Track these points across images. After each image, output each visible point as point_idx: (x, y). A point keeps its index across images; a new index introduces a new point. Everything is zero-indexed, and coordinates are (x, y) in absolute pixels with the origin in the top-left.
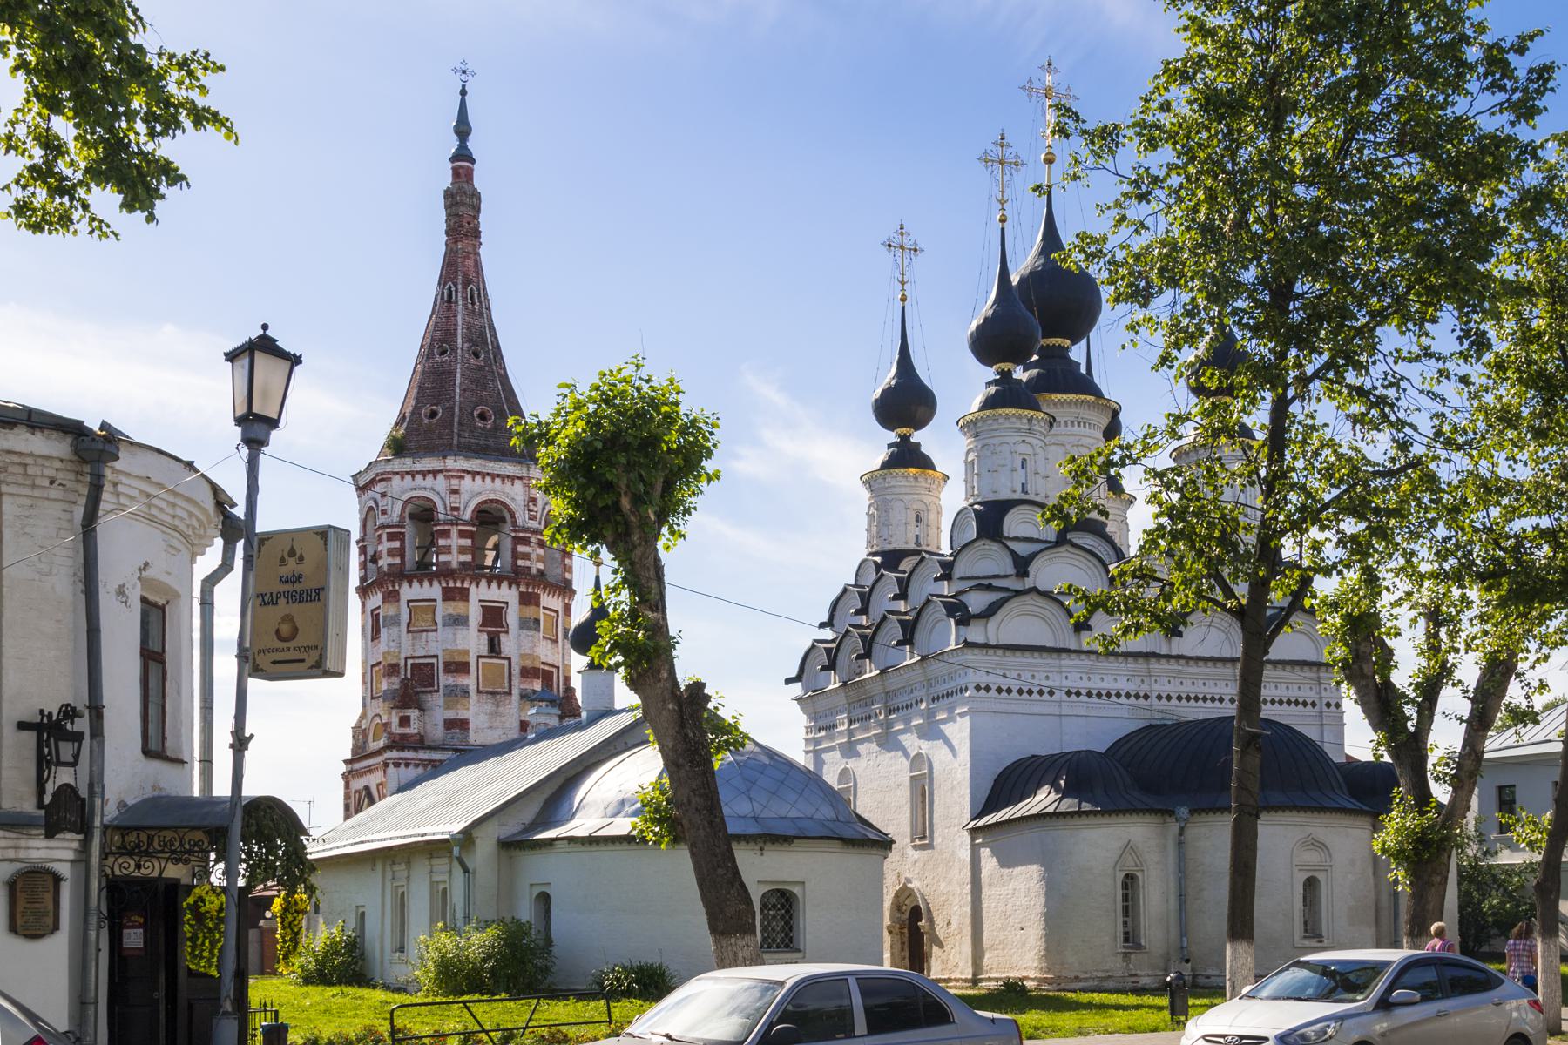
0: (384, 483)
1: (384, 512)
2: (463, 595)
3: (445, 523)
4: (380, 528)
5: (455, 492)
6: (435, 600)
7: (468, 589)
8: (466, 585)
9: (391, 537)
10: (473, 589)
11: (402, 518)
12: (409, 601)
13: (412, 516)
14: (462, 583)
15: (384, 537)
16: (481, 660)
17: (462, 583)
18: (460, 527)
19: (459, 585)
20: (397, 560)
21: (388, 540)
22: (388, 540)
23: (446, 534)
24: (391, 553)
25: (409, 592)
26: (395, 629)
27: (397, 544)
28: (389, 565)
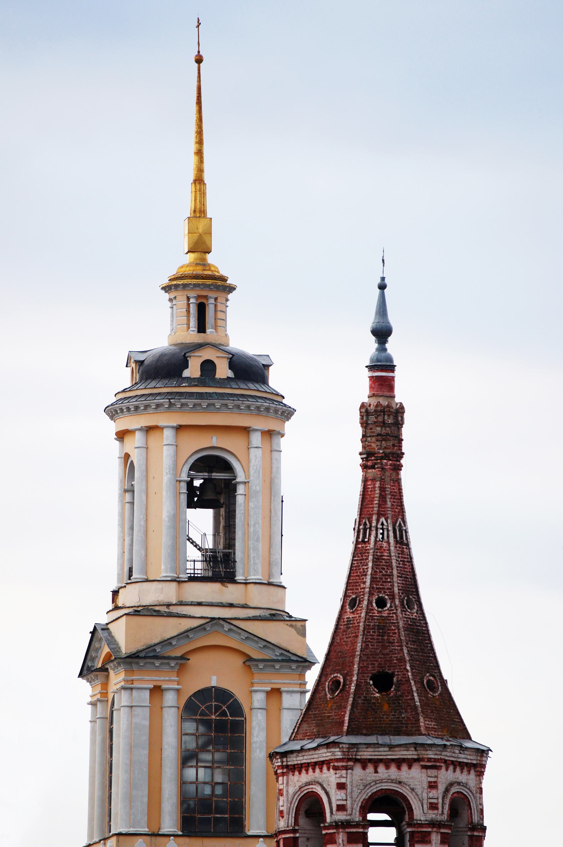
3: (330, 827)
5: (341, 786)
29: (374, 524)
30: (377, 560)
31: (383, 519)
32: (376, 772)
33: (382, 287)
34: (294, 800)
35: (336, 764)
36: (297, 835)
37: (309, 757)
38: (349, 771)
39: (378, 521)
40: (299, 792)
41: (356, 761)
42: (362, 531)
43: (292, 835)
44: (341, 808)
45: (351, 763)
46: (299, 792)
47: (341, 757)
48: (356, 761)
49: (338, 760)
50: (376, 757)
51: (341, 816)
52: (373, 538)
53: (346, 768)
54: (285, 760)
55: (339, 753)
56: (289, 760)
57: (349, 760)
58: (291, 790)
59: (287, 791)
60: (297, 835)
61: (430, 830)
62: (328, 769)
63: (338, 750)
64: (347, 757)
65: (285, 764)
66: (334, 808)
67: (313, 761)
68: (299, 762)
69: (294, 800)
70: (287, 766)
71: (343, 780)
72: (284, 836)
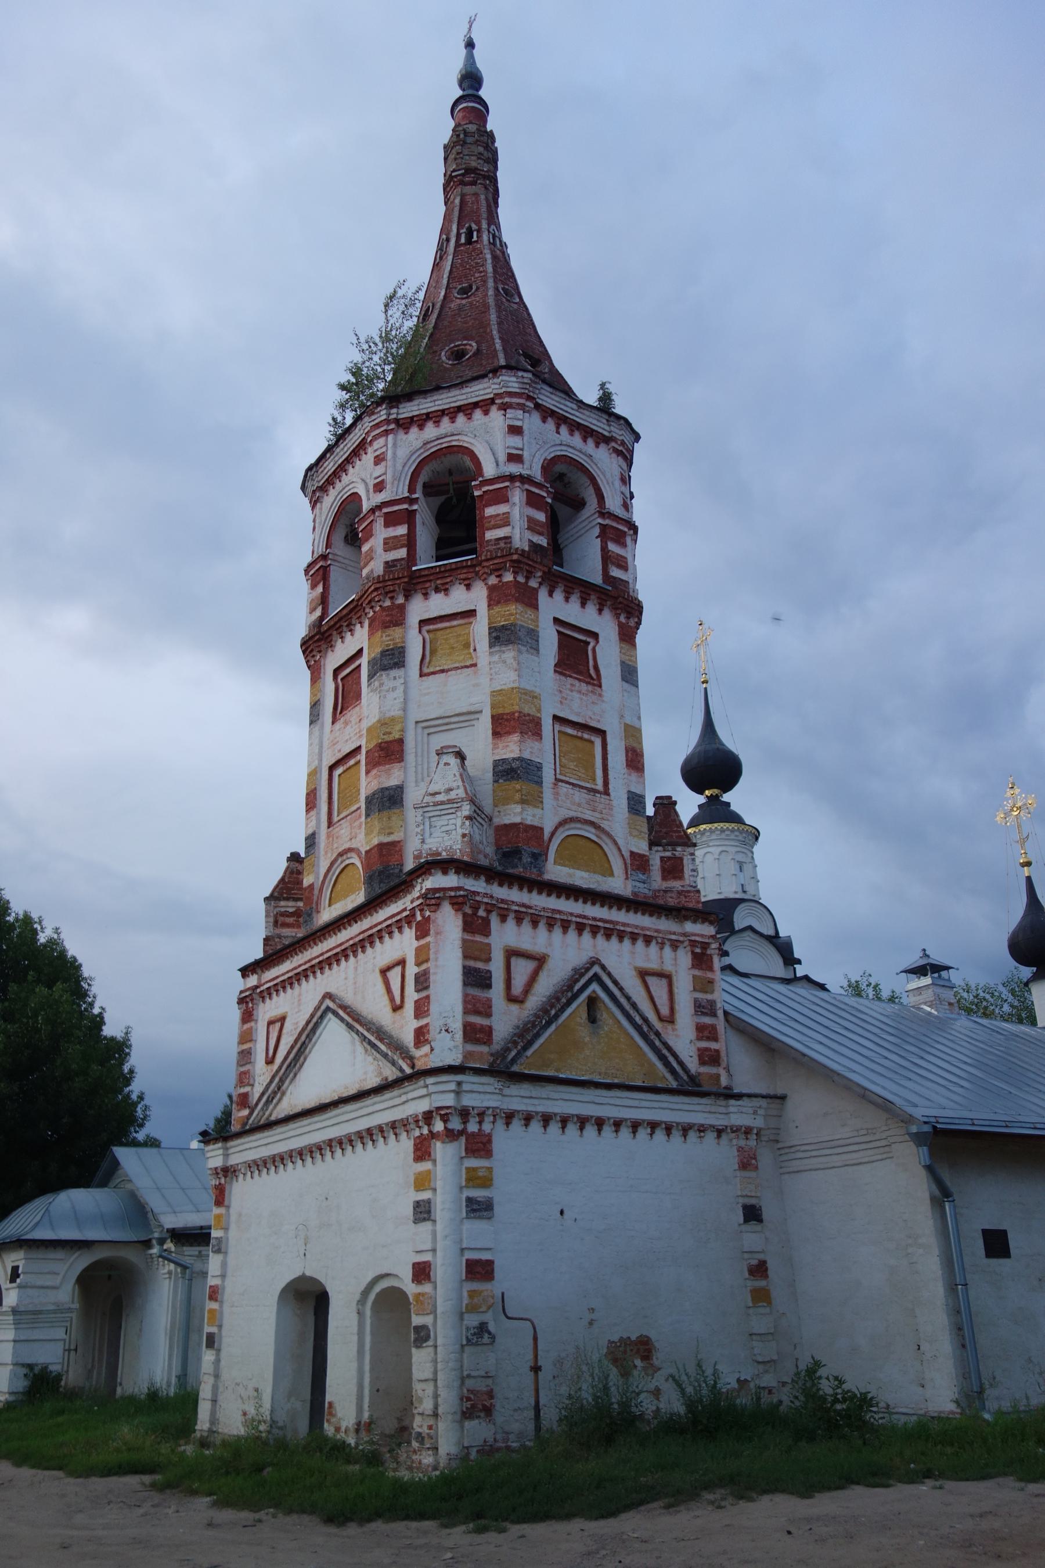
0: (381, 441)
1: (379, 487)
2: (530, 600)
4: (372, 511)
5: (515, 430)
6: (471, 613)
7: (535, 591)
8: (533, 583)
9: (391, 520)
10: (543, 595)
11: (412, 489)
12: (423, 623)
13: (430, 489)
14: (527, 578)
15: (380, 522)
16: (557, 727)
17: (527, 578)
18: (527, 486)
19: (521, 579)
20: (402, 553)
21: (387, 525)
22: (387, 525)
23: (500, 497)
24: (390, 544)
25: (419, 608)
26: (391, 679)
27: (402, 530)
28: (388, 565)
29: (484, 225)
30: (495, 258)
31: (493, 227)
32: (558, 433)
33: (470, 45)
34: (411, 461)
35: (507, 400)
36: (415, 507)
37: (448, 401)
38: (527, 415)
39: (489, 225)
40: (422, 451)
41: (538, 406)
42: (463, 236)
43: (405, 506)
44: (514, 458)
45: (531, 405)
46: (422, 451)
47: (518, 390)
48: (538, 406)
49: (511, 394)
50: (561, 412)
51: (514, 469)
52: (485, 237)
53: (522, 407)
54: (394, 411)
55: (516, 385)
56: (401, 411)
57: (529, 398)
58: (402, 453)
59: (394, 454)
60: (415, 507)
61: (626, 529)
62: (486, 413)
63: (514, 379)
64: (527, 391)
65: (392, 417)
66: (502, 457)
67: (453, 405)
68: (425, 411)
69: (411, 461)
70: (397, 421)
71: (519, 423)
72: (385, 510)
